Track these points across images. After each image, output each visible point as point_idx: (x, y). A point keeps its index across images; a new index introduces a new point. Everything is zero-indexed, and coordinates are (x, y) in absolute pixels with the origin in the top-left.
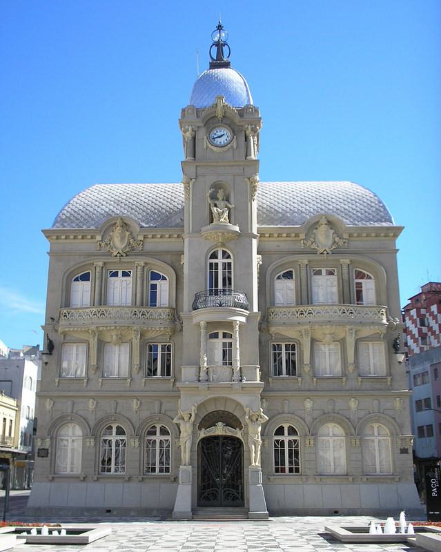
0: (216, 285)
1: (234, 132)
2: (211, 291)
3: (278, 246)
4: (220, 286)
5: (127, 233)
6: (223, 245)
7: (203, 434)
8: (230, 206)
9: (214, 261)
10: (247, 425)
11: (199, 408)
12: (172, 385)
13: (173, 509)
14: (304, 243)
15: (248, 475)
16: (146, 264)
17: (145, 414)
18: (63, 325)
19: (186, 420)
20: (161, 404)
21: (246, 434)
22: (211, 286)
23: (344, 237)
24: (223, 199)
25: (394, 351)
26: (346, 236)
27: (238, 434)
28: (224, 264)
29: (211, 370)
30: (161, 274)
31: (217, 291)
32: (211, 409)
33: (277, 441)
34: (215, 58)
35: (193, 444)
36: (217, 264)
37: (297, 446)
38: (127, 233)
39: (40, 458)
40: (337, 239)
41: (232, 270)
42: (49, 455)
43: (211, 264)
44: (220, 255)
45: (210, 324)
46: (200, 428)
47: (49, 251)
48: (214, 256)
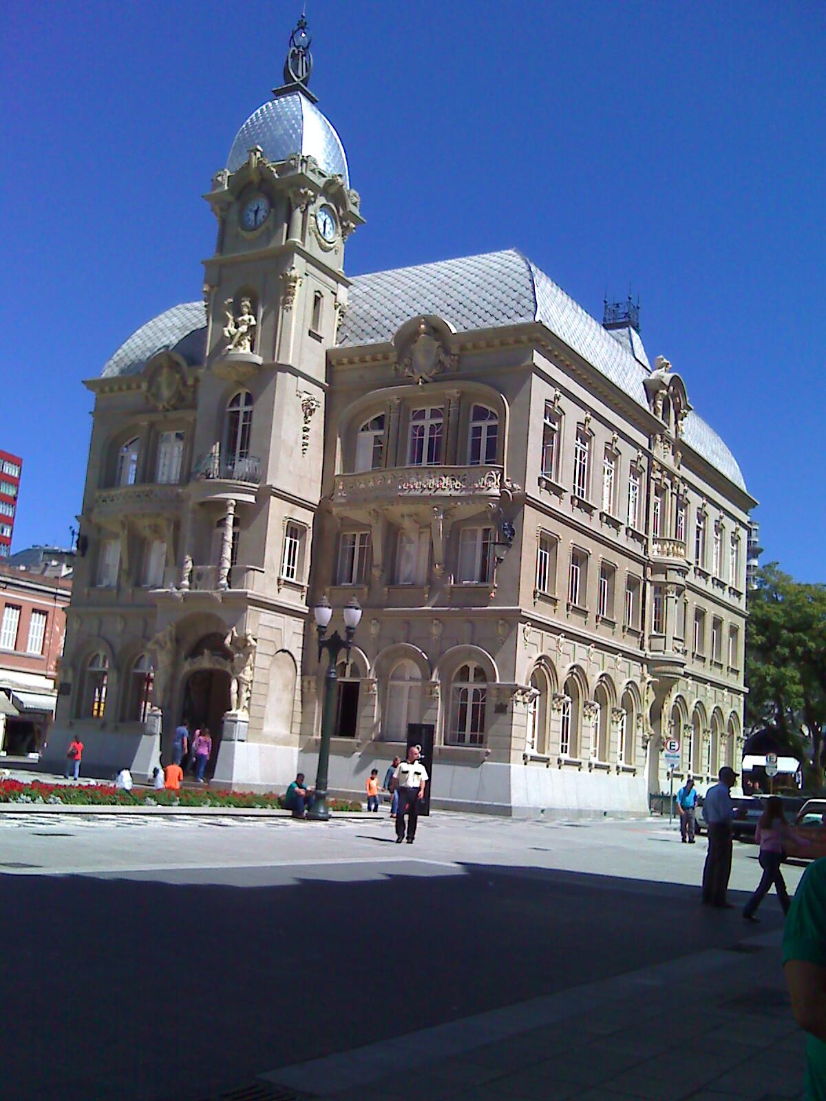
1: (272, 204)
5: (178, 376)
6: (240, 384)
7: (187, 667)
14: (396, 369)
18: (96, 518)
23: (453, 352)
29: (195, 573)
35: (173, 678)
38: (178, 376)
40: (442, 357)
42: (71, 693)
46: (186, 659)
47: (92, 410)
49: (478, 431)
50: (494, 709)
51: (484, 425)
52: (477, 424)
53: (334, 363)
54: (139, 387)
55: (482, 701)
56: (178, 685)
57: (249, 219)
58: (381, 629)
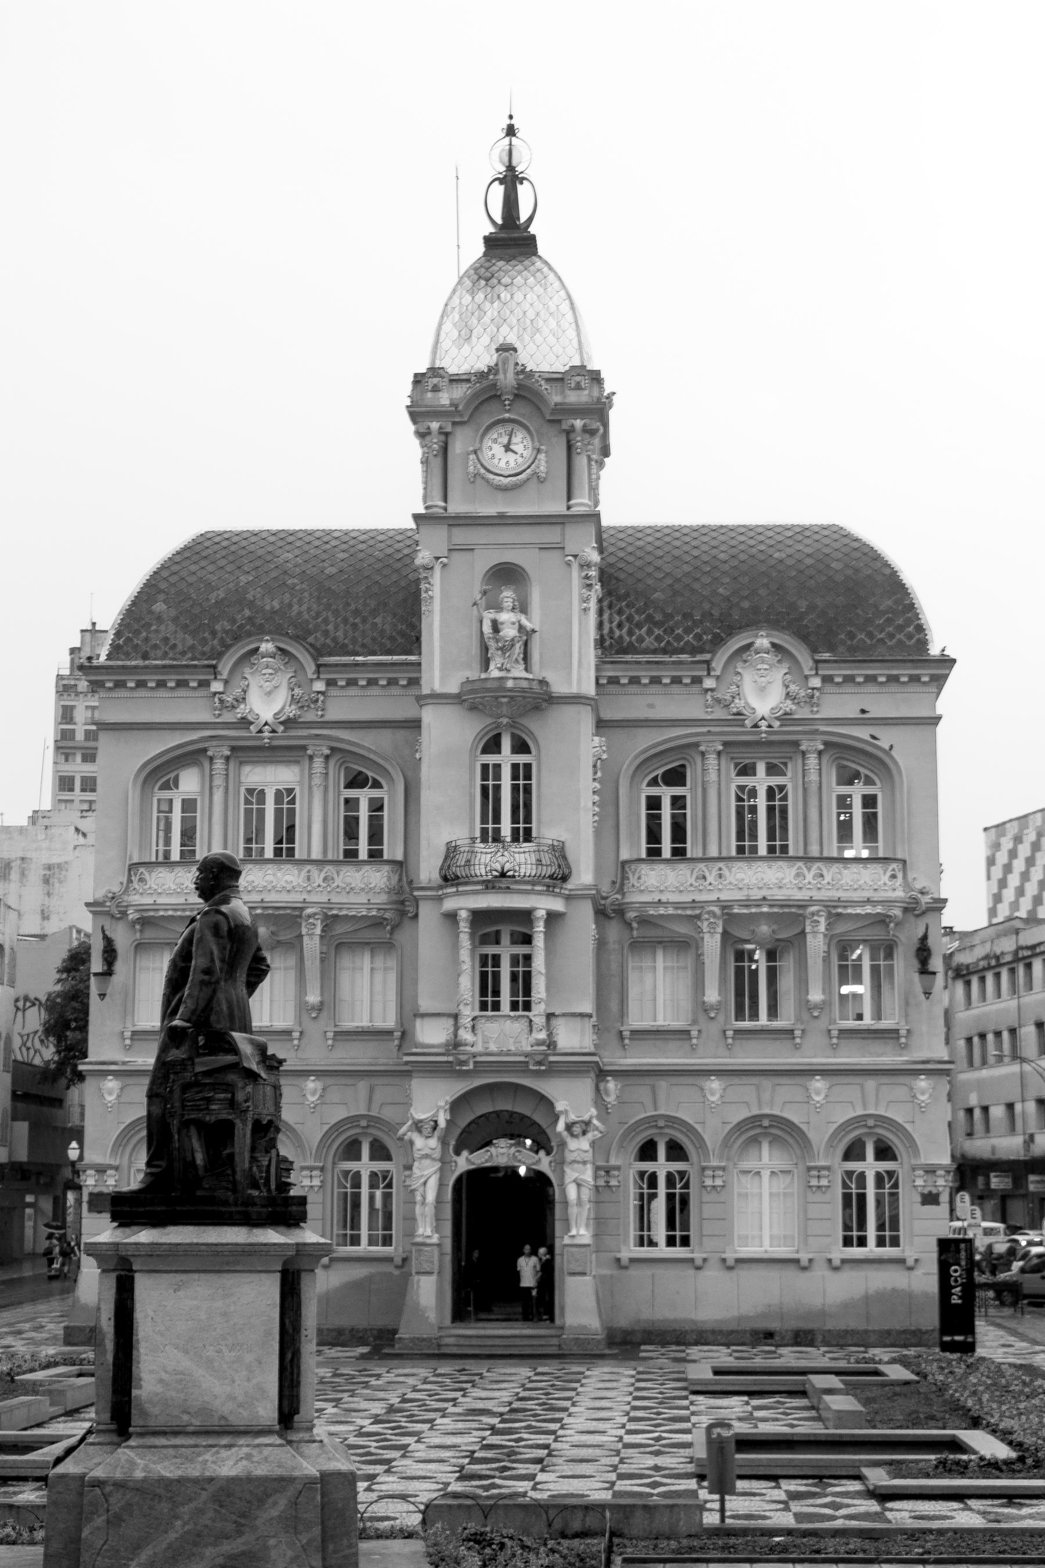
0: (497, 819)
2: (484, 832)
3: (651, 706)
4: (506, 827)
7: (464, 1163)
8: (528, 625)
9: (491, 759)
10: (563, 1144)
11: (456, 1106)
12: (396, 1042)
13: (395, 1332)
15: (562, 1255)
16: (333, 749)
17: (340, 1114)
19: (425, 1132)
20: (372, 1090)
21: (560, 1164)
22: (484, 820)
24: (513, 609)
25: (916, 964)
26: (816, 682)
27: (544, 1163)
28: (515, 767)
30: (370, 774)
31: (497, 831)
32: (484, 1108)
33: (642, 1174)
34: (499, 221)
35: (441, 1185)
36: (498, 767)
37: (686, 1186)
39: (95, 1215)
41: (534, 782)
43: (485, 767)
44: (506, 744)
45: (479, 917)
46: (458, 1153)
48: (493, 745)
49: (843, 802)
50: (919, 1199)
51: (857, 792)
52: (844, 790)
53: (604, 681)
54: (204, 684)
55: (891, 1188)
56: (449, 1195)
57: (493, 455)
58: (724, 1090)
